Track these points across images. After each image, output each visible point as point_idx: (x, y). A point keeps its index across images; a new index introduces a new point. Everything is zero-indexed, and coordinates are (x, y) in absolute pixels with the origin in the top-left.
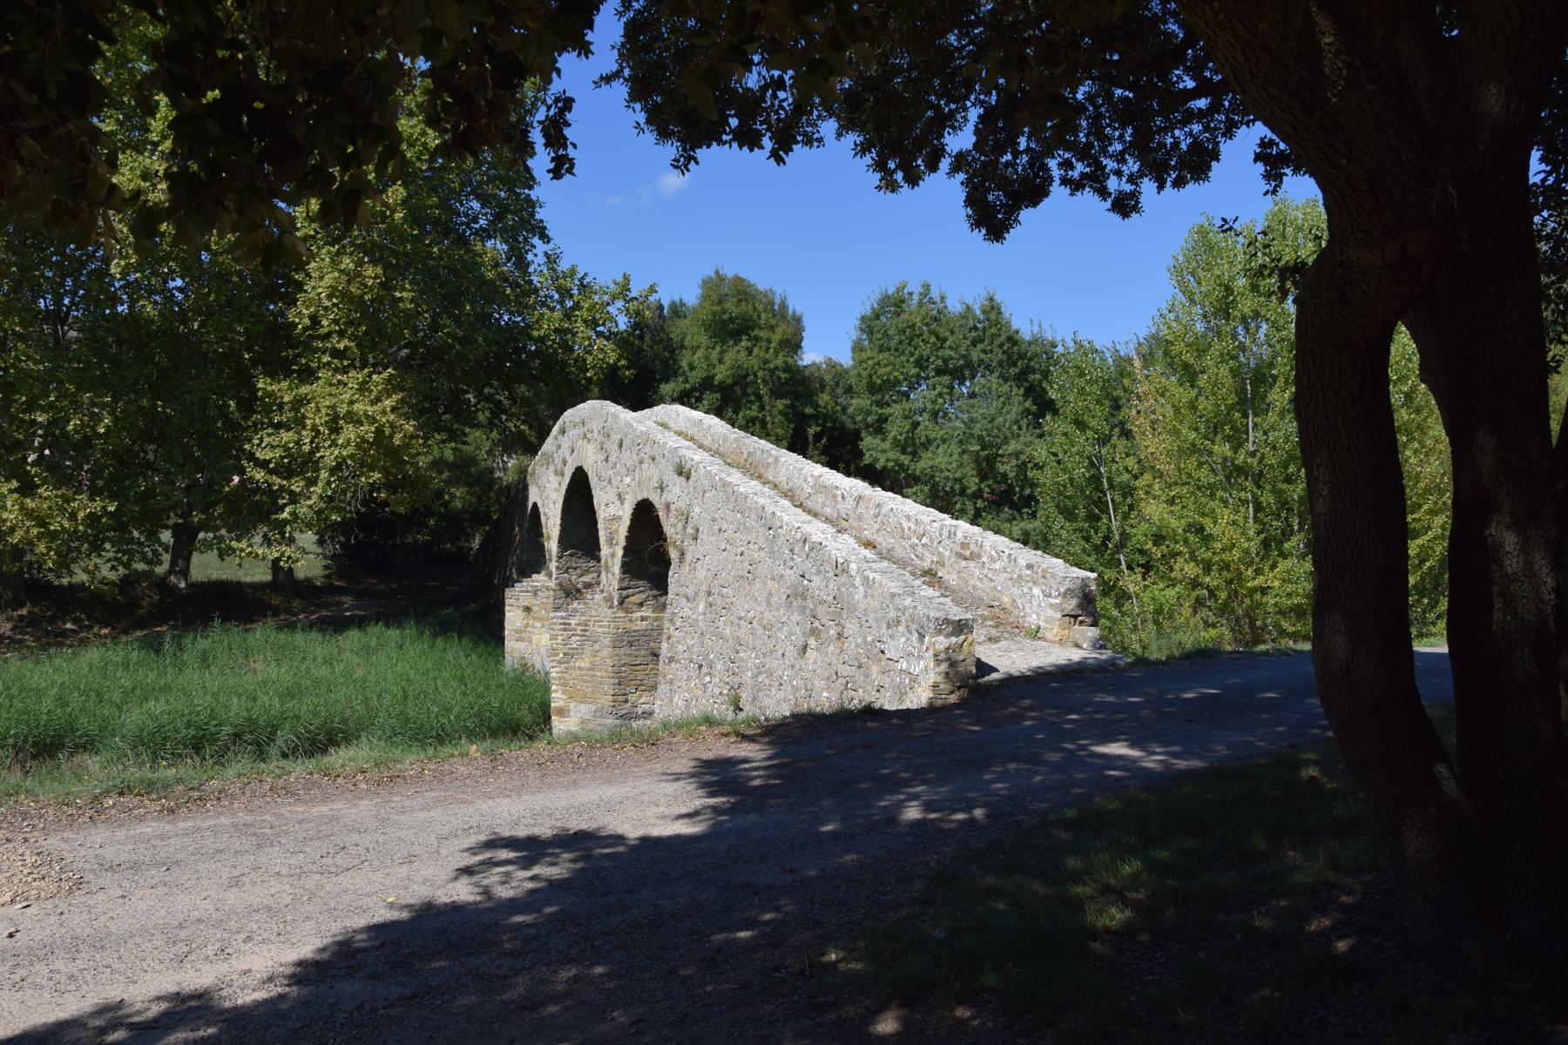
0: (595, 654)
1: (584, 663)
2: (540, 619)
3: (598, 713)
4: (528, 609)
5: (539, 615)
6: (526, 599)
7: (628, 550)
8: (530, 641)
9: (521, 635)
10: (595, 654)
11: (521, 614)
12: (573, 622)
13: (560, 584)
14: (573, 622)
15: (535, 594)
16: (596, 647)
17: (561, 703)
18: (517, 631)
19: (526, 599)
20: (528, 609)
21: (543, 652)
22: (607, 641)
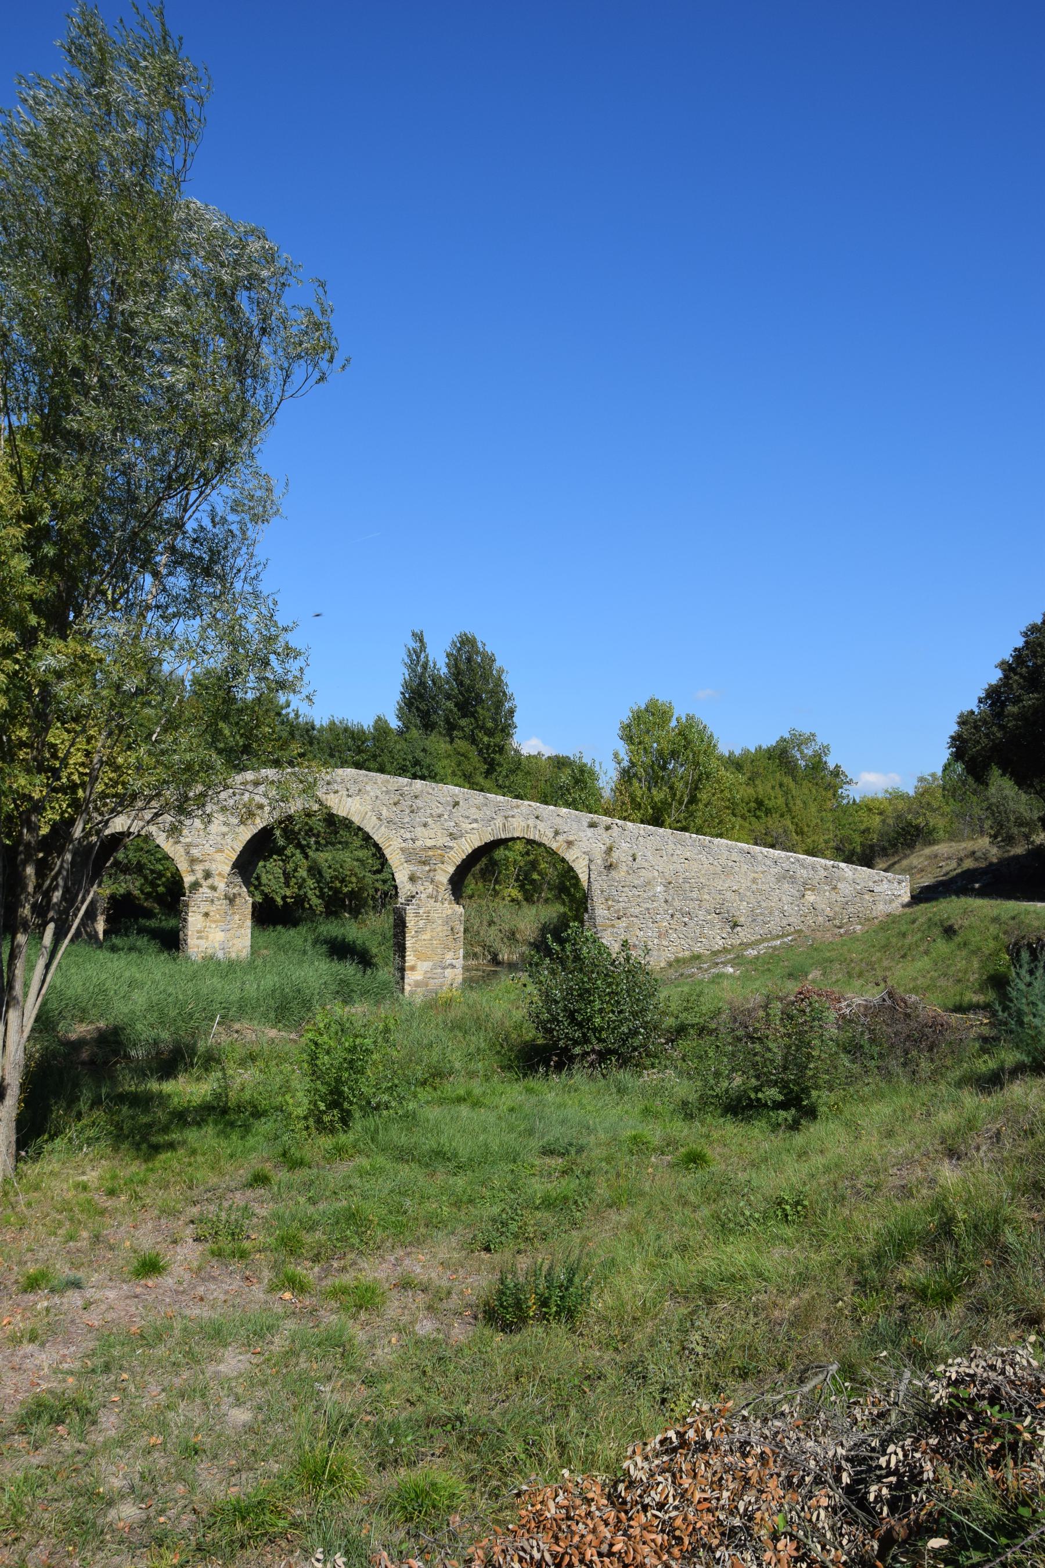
0: (433, 929)
1: (427, 936)
2: (215, 922)
3: (434, 968)
4: (206, 915)
5: (215, 918)
6: (205, 907)
7: (458, 867)
8: (207, 938)
9: (201, 934)
10: (433, 929)
11: (200, 917)
12: (421, 911)
13: (225, 895)
14: (421, 911)
15: (212, 901)
16: (434, 926)
17: (413, 963)
18: (198, 932)
19: (205, 907)
20: (206, 915)
21: (217, 945)
22: (440, 922)
